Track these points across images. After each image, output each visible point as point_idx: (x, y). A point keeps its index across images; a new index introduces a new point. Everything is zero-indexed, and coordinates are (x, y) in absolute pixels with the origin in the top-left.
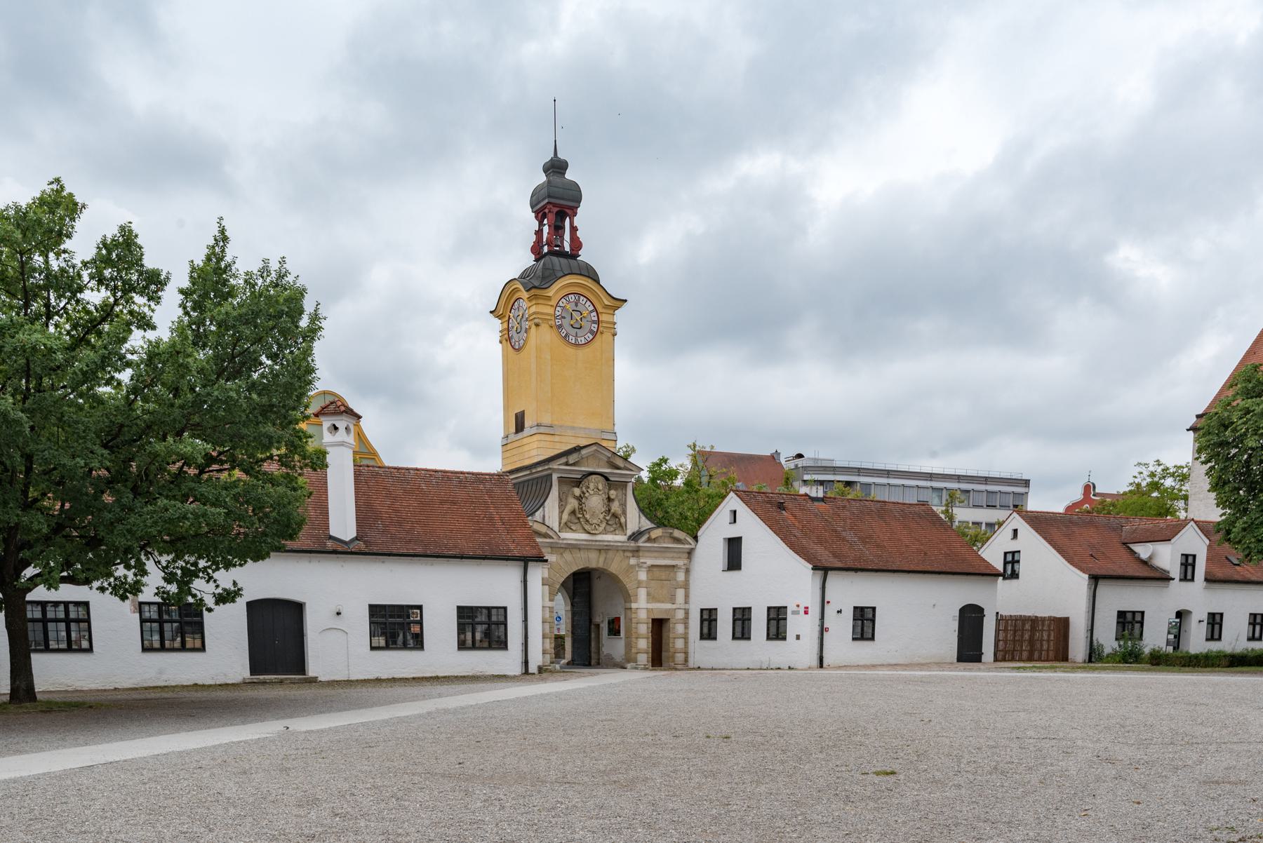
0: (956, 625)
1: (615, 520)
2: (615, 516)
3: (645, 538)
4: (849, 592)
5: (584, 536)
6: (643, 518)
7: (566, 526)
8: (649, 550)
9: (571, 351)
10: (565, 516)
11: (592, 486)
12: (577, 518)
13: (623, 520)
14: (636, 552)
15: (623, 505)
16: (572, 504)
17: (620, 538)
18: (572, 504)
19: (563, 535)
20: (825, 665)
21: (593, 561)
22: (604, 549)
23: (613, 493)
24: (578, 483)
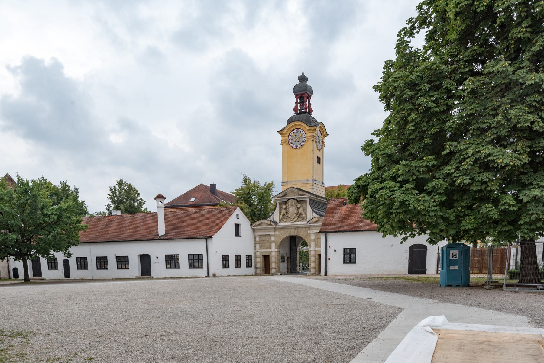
0: (407, 255)
1: (300, 216)
2: (300, 214)
3: (310, 222)
4: (338, 242)
5: (289, 223)
6: (314, 214)
7: (281, 220)
8: (314, 227)
9: (295, 151)
10: (281, 217)
11: (290, 204)
12: (284, 217)
13: (304, 215)
14: (309, 228)
15: (305, 209)
16: (284, 211)
17: (304, 222)
18: (284, 211)
19: (280, 224)
20: (328, 274)
21: (293, 233)
22: (297, 228)
23: (299, 206)
24: (285, 203)
